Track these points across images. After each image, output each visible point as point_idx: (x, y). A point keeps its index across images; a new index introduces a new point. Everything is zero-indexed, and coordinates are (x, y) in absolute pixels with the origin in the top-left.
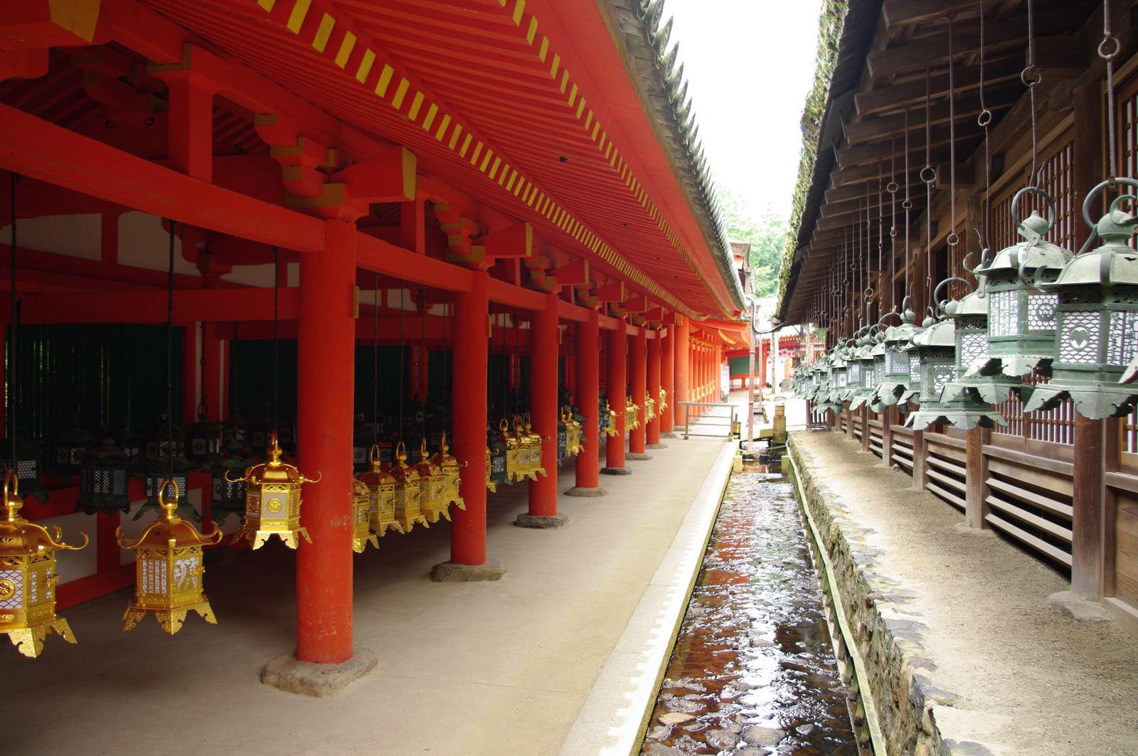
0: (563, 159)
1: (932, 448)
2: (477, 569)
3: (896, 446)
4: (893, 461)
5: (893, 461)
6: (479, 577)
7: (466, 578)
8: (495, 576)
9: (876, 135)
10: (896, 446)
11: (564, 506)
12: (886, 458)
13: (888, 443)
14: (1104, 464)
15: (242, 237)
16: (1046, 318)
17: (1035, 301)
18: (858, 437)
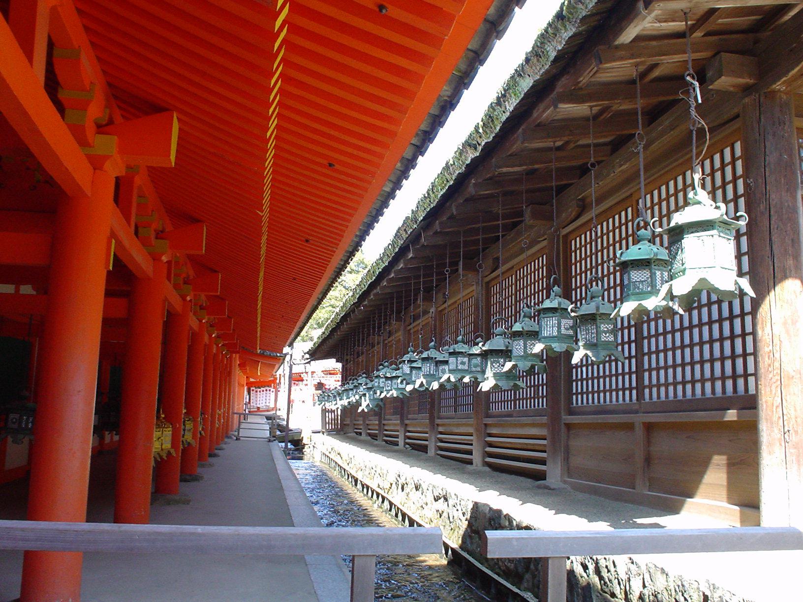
0: (307, 241)
1: (441, 429)
2: (177, 498)
3: (408, 434)
4: (406, 443)
5: (406, 443)
6: (177, 502)
7: (168, 503)
8: (187, 502)
9: (439, 241)
10: (408, 434)
11: (199, 470)
12: (401, 443)
13: (403, 433)
14: (563, 413)
15: (130, 267)
16: (567, 329)
17: (563, 322)
18: (369, 435)
